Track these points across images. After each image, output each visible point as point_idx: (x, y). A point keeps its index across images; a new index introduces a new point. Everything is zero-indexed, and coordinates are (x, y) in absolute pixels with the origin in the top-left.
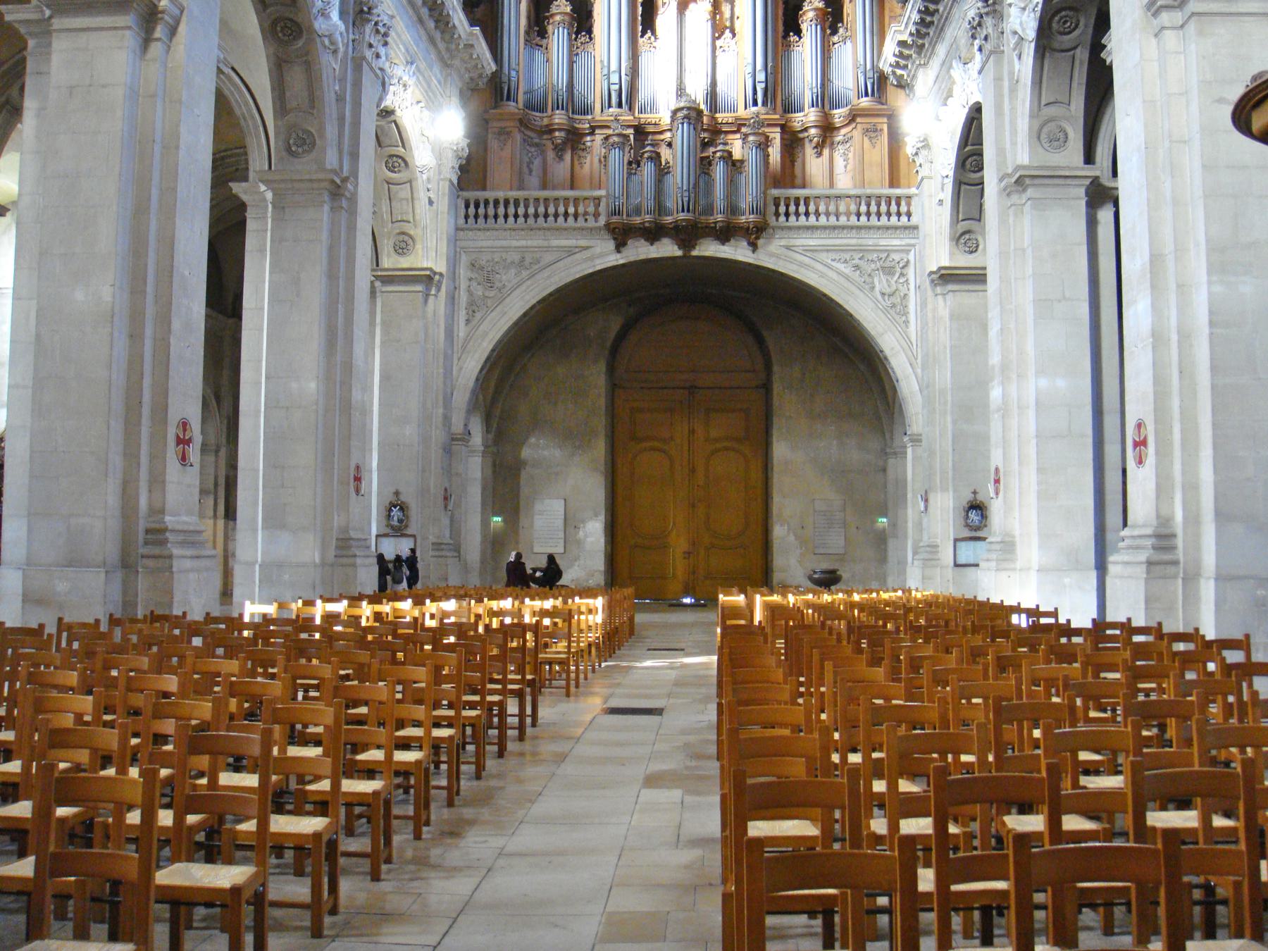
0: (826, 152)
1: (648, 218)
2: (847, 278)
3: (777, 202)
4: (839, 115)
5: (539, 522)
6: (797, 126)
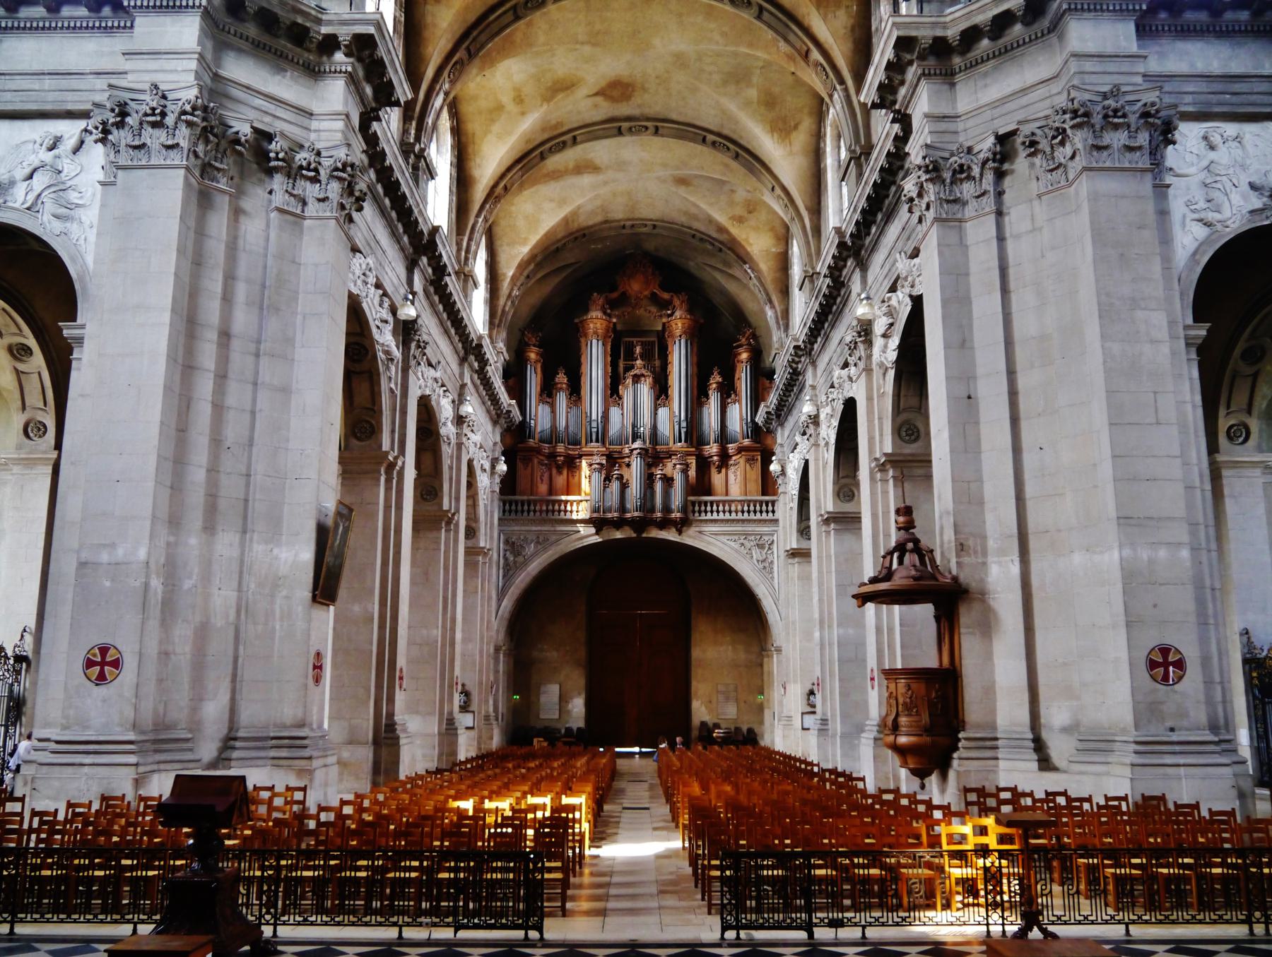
0: (724, 470)
1: (616, 515)
2: (736, 551)
3: (693, 503)
4: (732, 447)
5: (543, 699)
6: (706, 454)
